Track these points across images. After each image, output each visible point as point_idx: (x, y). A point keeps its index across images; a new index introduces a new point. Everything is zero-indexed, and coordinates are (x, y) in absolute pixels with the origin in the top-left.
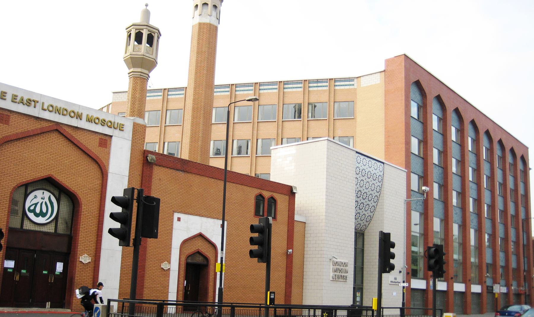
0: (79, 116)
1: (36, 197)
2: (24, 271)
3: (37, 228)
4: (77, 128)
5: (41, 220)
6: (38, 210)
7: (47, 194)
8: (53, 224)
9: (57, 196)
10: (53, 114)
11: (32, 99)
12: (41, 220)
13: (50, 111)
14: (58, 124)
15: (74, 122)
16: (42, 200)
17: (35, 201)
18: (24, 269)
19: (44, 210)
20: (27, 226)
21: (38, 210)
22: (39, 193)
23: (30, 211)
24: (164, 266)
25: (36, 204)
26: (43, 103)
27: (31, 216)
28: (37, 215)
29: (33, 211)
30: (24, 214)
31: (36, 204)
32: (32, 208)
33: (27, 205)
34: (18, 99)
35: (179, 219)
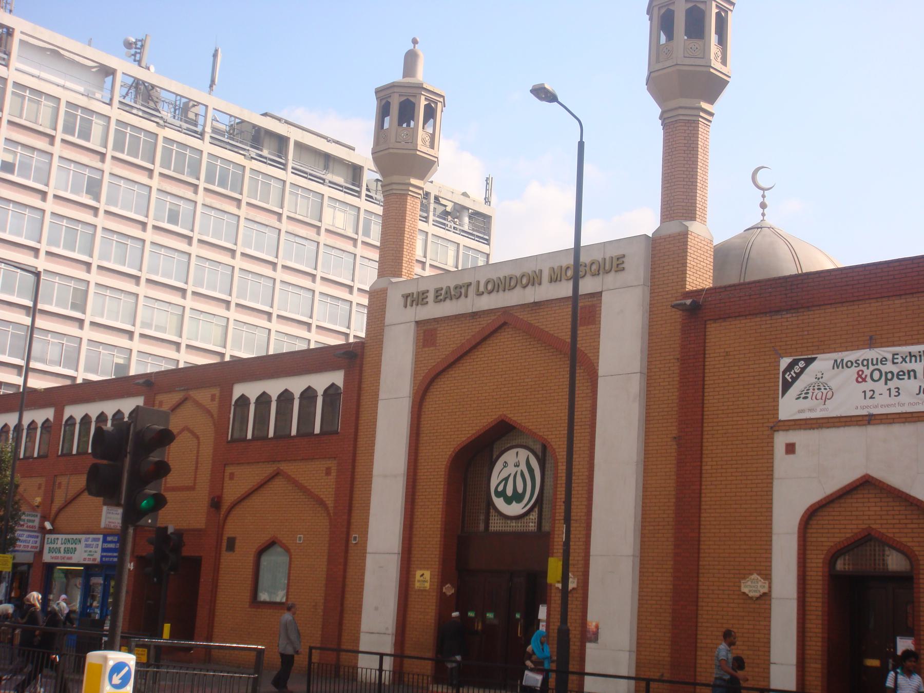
0: (533, 279)
1: (506, 464)
2: (490, 615)
3: (513, 526)
4: (536, 306)
5: (515, 509)
6: (509, 492)
7: (523, 454)
8: (534, 516)
9: (540, 454)
10: (494, 294)
11: (460, 283)
12: (515, 509)
13: (490, 292)
14: (506, 311)
15: (530, 295)
16: (516, 469)
17: (504, 475)
18: (490, 612)
19: (520, 489)
20: (496, 525)
21: (509, 492)
22: (509, 457)
23: (498, 494)
24: (752, 586)
25: (506, 479)
26: (478, 282)
27: (499, 503)
28: (508, 501)
29: (501, 494)
30: (490, 504)
31: (506, 479)
32: (500, 488)
33: (494, 482)
34: (443, 292)
35: (790, 449)
